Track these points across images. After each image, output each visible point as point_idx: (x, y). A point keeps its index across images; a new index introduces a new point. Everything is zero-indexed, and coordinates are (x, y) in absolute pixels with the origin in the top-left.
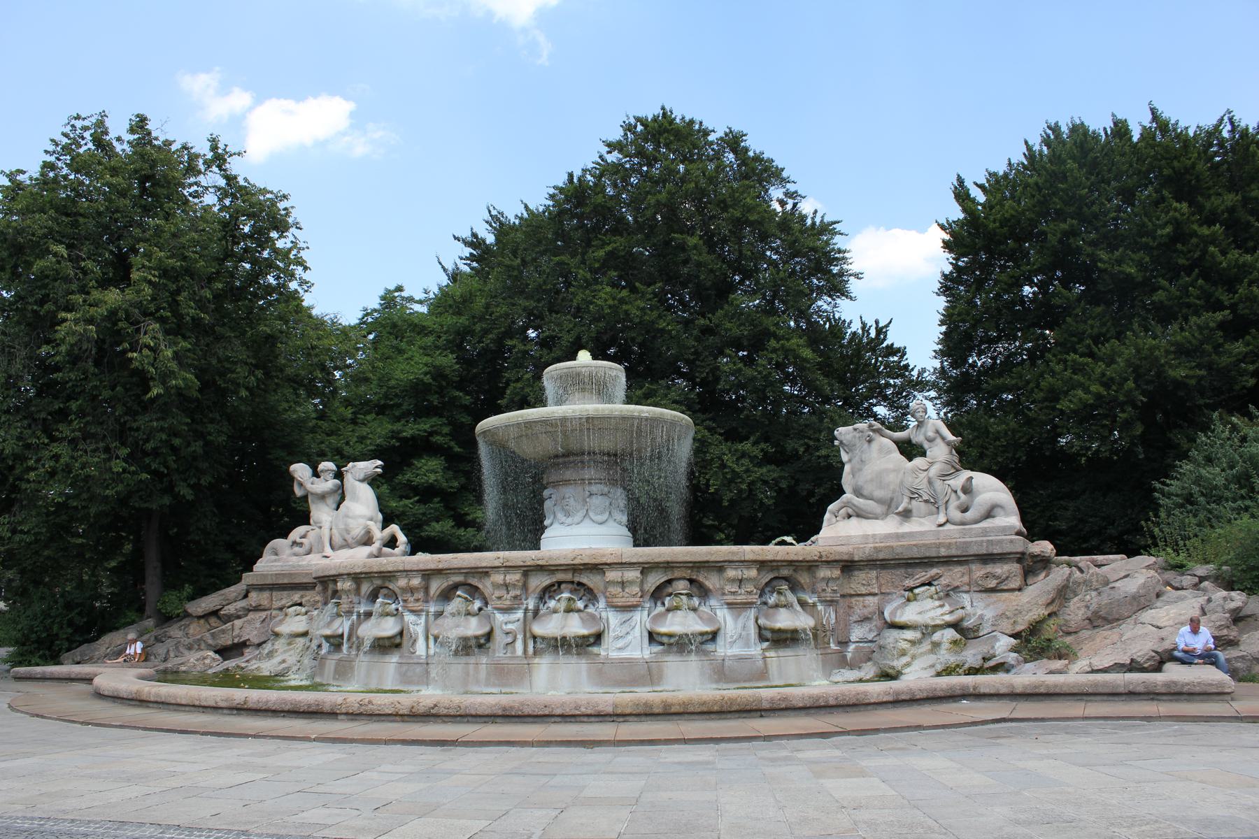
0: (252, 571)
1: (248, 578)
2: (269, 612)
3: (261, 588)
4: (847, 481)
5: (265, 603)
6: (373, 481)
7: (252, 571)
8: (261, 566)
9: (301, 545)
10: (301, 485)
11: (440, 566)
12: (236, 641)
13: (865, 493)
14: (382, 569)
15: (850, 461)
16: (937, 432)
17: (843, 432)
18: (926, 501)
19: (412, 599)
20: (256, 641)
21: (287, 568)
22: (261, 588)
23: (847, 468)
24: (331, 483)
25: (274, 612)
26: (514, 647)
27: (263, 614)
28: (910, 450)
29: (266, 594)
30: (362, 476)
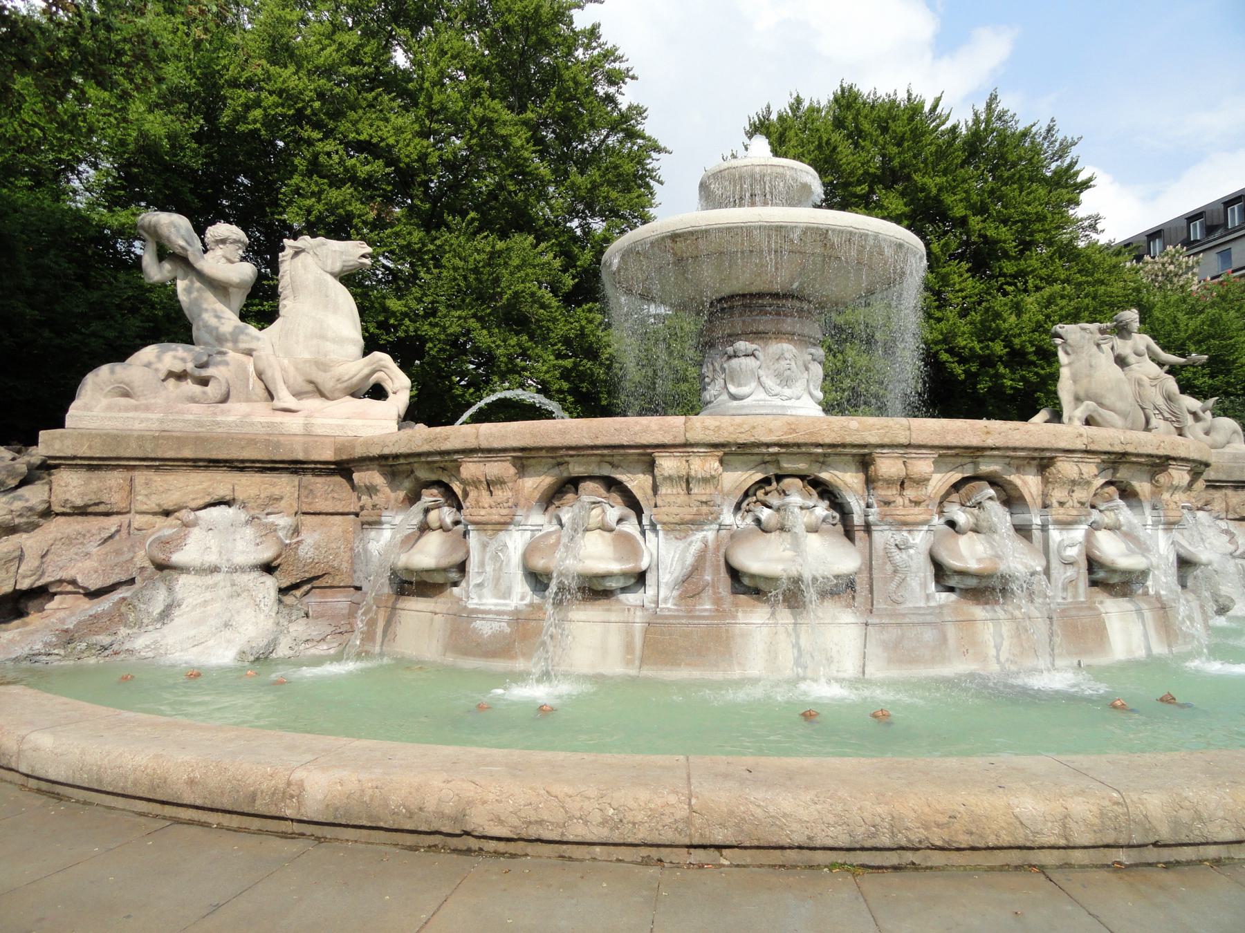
0: (61, 424)
1: (49, 443)
2: (124, 519)
3: (94, 465)
4: (1065, 389)
5: (116, 499)
6: (350, 279)
7: (61, 424)
8: (76, 414)
9: (204, 382)
10: (164, 253)
11: (990, 442)
12: (24, 585)
13: (1107, 402)
14: (848, 440)
15: (1070, 364)
16: (1148, 348)
17: (1069, 330)
18: (1166, 419)
19: (899, 500)
20: (93, 585)
21: (180, 426)
22: (94, 465)
23: (1065, 372)
24: (246, 271)
25: (138, 521)
26: (1076, 587)
27: (112, 523)
28: (1121, 361)
29: (115, 479)
30: (337, 267)
